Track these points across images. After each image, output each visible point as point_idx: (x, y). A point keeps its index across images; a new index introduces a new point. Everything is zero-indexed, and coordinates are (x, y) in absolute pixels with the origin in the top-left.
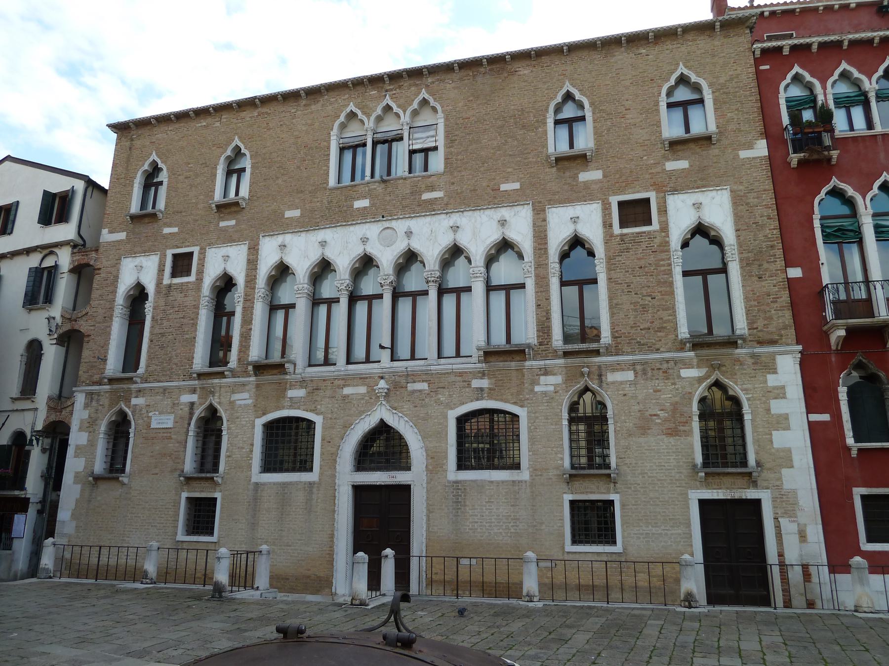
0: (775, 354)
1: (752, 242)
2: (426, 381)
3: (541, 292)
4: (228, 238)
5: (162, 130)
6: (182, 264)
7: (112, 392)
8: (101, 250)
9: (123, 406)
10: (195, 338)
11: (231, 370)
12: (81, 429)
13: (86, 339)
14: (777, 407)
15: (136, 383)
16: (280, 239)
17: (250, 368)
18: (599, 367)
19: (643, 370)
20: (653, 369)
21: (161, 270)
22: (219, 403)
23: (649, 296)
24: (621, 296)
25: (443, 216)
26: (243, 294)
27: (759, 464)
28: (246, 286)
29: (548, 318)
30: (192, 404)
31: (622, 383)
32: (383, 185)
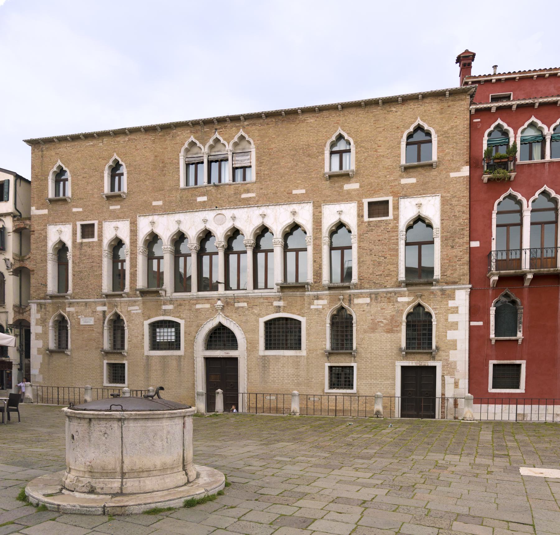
1: (451, 226)
2: (246, 302)
3: (317, 253)
4: (116, 216)
5: (62, 145)
6: (88, 230)
7: (53, 304)
8: (33, 219)
9: (61, 312)
10: (101, 274)
11: (127, 294)
12: (37, 324)
13: (32, 273)
14: (452, 318)
15: (68, 299)
16: (150, 218)
17: (138, 292)
18: (350, 295)
19: (375, 297)
20: (382, 297)
21: (74, 234)
22: (121, 312)
23: (383, 257)
24: (366, 256)
26: (129, 250)
27: (437, 348)
28: (131, 245)
29: (321, 268)
30: (104, 312)
31: (362, 304)
32: (215, 188)
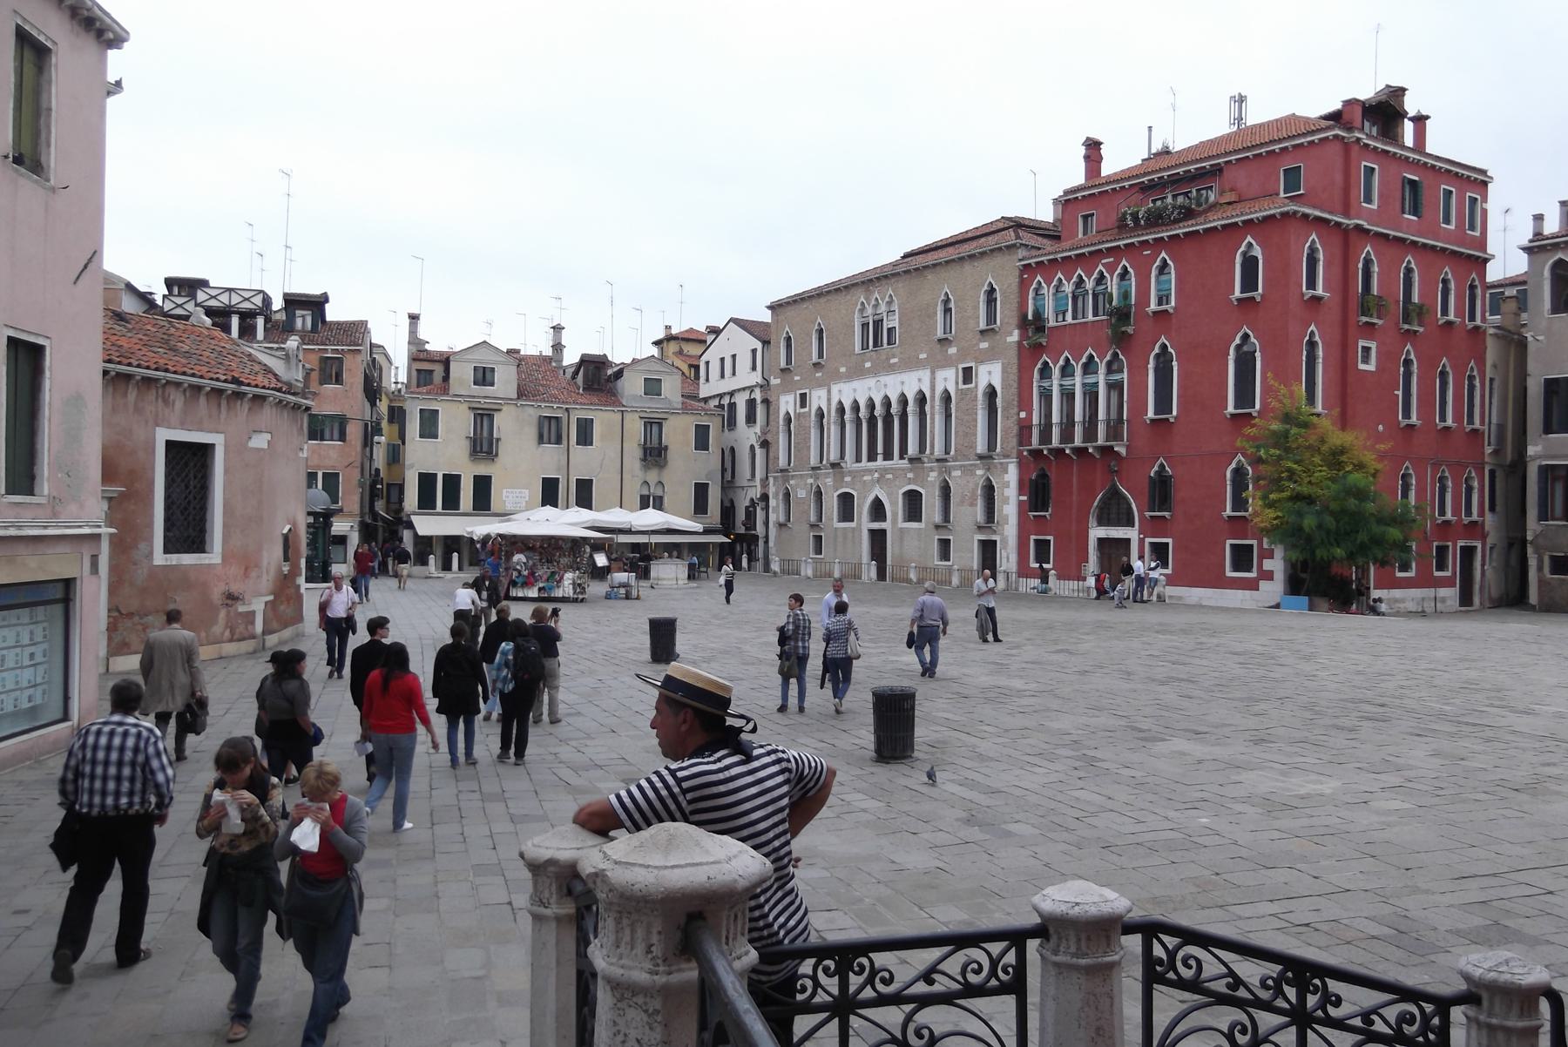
0: (1008, 463)
7: (783, 477)
11: (824, 466)
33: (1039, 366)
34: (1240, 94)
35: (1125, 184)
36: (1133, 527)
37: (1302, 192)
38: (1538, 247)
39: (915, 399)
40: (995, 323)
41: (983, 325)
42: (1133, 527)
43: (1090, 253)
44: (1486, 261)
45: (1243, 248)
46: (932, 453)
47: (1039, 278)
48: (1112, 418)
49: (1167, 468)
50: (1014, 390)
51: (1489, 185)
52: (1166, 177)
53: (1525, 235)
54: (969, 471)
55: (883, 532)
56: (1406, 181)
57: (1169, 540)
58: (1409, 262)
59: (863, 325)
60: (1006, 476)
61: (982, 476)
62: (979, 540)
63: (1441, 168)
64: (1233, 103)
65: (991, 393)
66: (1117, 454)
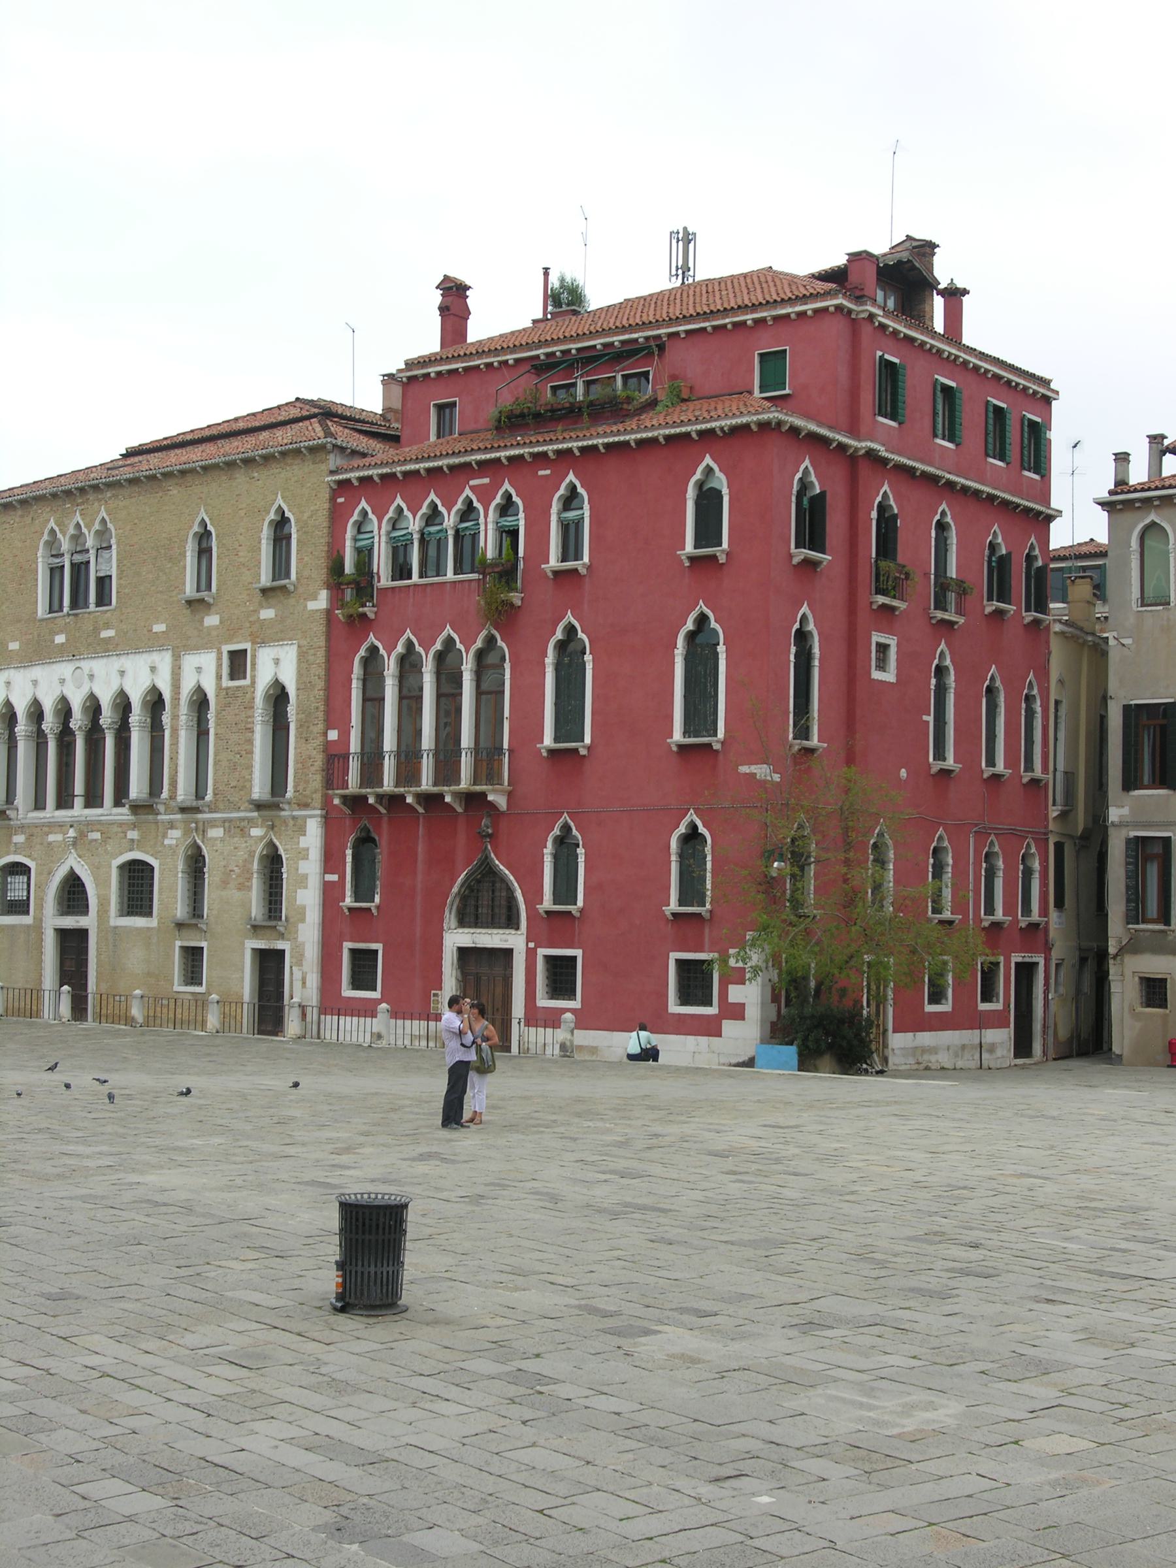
0: (305, 817)
2: (98, 831)
25: (115, 657)
33: (362, 652)
34: (685, 229)
35: (508, 357)
36: (518, 928)
37: (787, 391)
38: (1122, 502)
39: (145, 703)
40: (288, 576)
41: (265, 579)
42: (518, 928)
43: (451, 468)
44: (1049, 518)
45: (698, 476)
46: (173, 797)
47: (363, 504)
48: (482, 745)
49: (575, 832)
50: (318, 692)
51: (1054, 403)
52: (573, 352)
53: (1104, 485)
54: (238, 828)
55: (83, 934)
56: (939, 388)
57: (578, 953)
58: (943, 513)
59: (52, 570)
60: (302, 838)
61: (262, 838)
62: (253, 949)
63: (987, 371)
64: (674, 242)
65: (279, 697)
66: (492, 806)
